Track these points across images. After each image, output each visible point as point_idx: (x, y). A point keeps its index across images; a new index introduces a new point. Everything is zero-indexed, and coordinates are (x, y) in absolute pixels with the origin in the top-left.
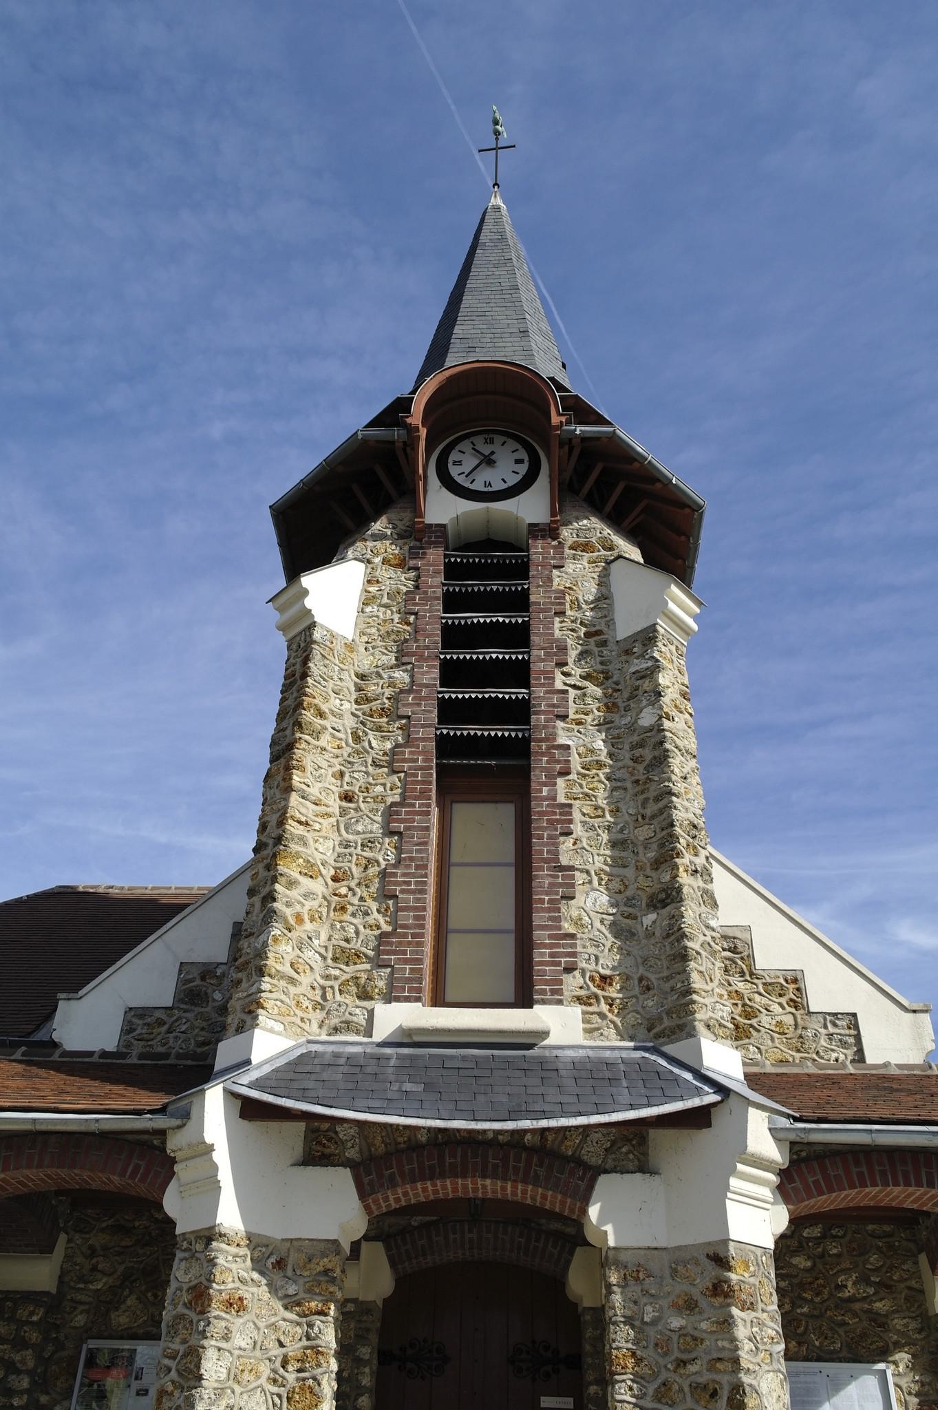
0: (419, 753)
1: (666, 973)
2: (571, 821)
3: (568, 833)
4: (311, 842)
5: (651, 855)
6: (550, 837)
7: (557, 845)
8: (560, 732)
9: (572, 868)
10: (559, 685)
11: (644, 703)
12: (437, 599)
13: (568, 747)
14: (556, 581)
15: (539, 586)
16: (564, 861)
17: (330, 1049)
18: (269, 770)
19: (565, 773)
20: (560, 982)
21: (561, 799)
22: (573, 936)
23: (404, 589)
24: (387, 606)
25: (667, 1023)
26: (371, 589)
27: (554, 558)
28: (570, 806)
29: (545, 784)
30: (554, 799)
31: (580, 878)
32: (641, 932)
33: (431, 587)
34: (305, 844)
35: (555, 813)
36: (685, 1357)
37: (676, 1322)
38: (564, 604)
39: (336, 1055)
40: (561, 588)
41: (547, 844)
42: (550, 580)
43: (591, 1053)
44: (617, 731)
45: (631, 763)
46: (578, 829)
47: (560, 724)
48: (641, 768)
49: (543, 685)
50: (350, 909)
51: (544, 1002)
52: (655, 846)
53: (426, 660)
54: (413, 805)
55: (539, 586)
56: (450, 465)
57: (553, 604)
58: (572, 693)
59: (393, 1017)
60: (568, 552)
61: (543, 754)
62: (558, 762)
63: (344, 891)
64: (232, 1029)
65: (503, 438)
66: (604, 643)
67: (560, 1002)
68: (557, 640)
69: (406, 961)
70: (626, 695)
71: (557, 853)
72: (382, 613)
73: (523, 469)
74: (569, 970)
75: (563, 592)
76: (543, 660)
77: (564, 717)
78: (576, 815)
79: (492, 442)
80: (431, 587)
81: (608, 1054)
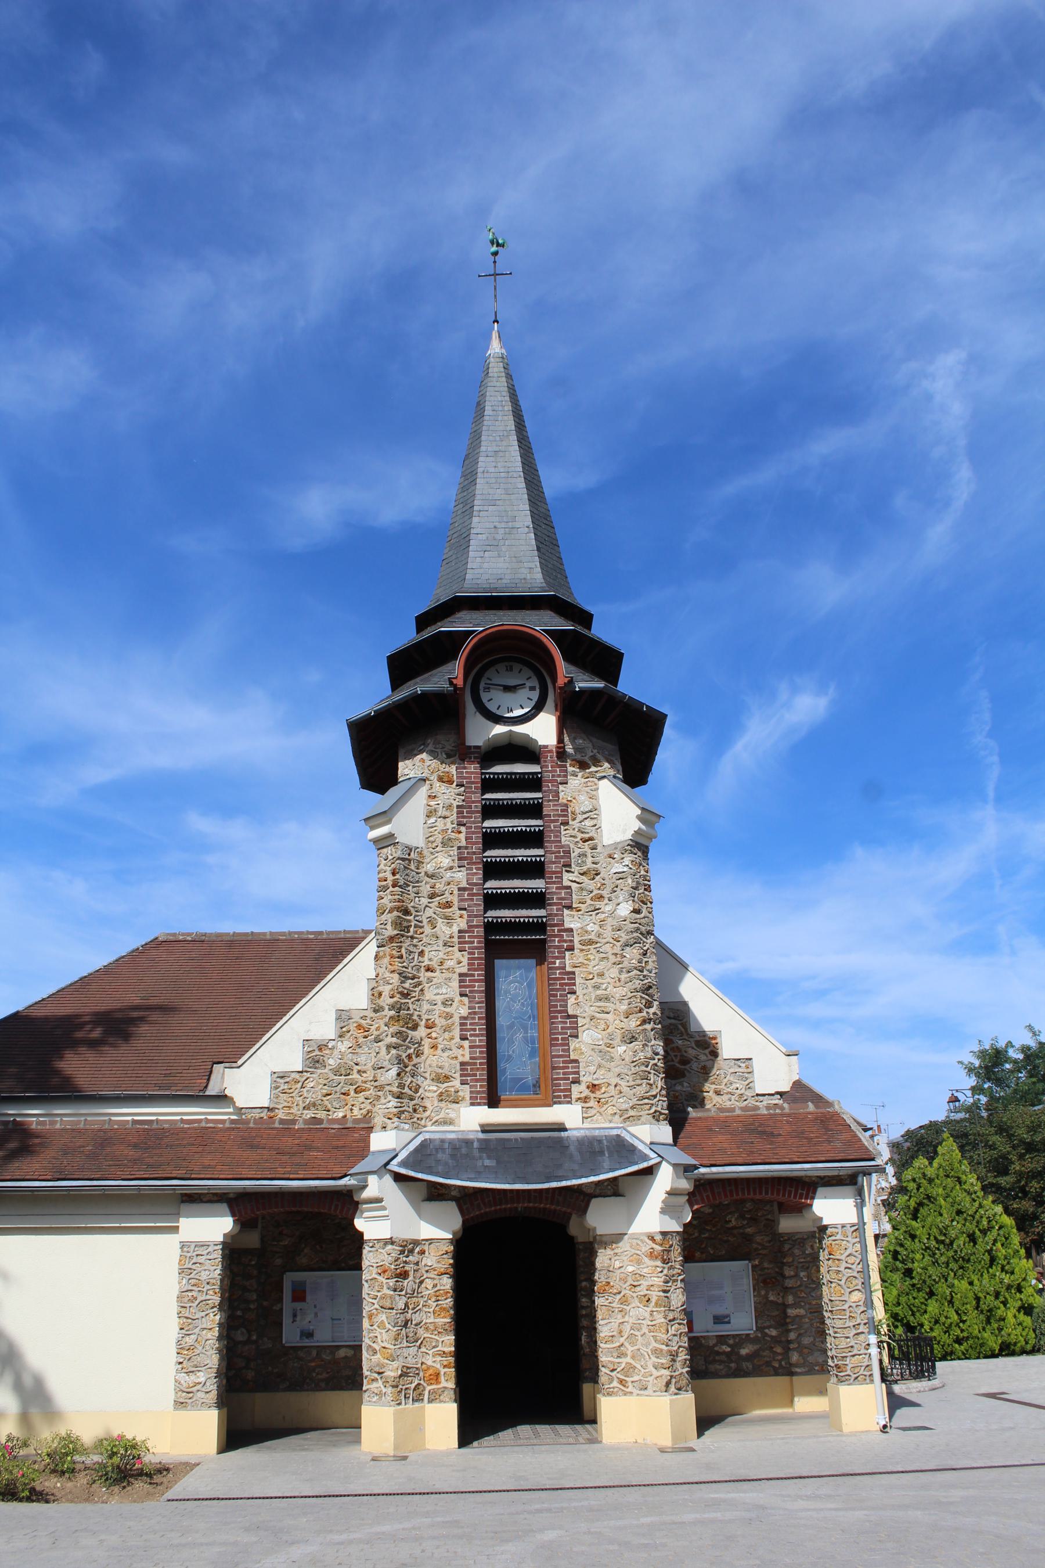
0: (475, 937)
1: (632, 1083)
2: (574, 984)
3: (574, 993)
4: (411, 1006)
5: (624, 1007)
6: (561, 995)
7: (566, 1001)
8: (567, 919)
9: (576, 1017)
10: (566, 883)
11: (621, 898)
12: (477, 812)
13: (571, 930)
14: (561, 795)
15: (550, 801)
16: (570, 1012)
17: (437, 1136)
18: (377, 952)
19: (571, 949)
20: (570, 1090)
21: (568, 969)
22: (576, 1061)
23: (455, 804)
24: (445, 818)
25: (631, 1113)
26: (432, 803)
27: (559, 776)
28: (573, 973)
29: (557, 958)
30: (564, 968)
31: (581, 1022)
32: (617, 1057)
33: (474, 802)
34: (409, 1009)
35: (564, 979)
36: (636, 1283)
37: (630, 1269)
38: (567, 816)
39: (443, 1141)
40: (565, 801)
41: (559, 1001)
42: (557, 794)
43: (588, 1133)
44: (603, 916)
45: (612, 941)
46: (578, 989)
47: (566, 912)
48: (618, 944)
49: (554, 883)
50: (440, 1047)
51: (560, 1103)
52: (626, 1002)
53: (475, 863)
54: (473, 975)
55: (550, 801)
56: (481, 692)
57: (559, 816)
58: (574, 886)
59: (472, 1118)
60: (570, 769)
61: (556, 936)
62: (565, 941)
63: (434, 1035)
64: (378, 1127)
65: (519, 666)
66: (594, 848)
67: (569, 1102)
68: (562, 847)
69: (477, 1081)
70: (609, 889)
71: (566, 1006)
72: (440, 824)
73: (535, 695)
74: (577, 1081)
75: (566, 805)
76: (554, 863)
77: (569, 907)
78: (578, 980)
79: (511, 670)
80: (474, 802)
81: (597, 1133)
